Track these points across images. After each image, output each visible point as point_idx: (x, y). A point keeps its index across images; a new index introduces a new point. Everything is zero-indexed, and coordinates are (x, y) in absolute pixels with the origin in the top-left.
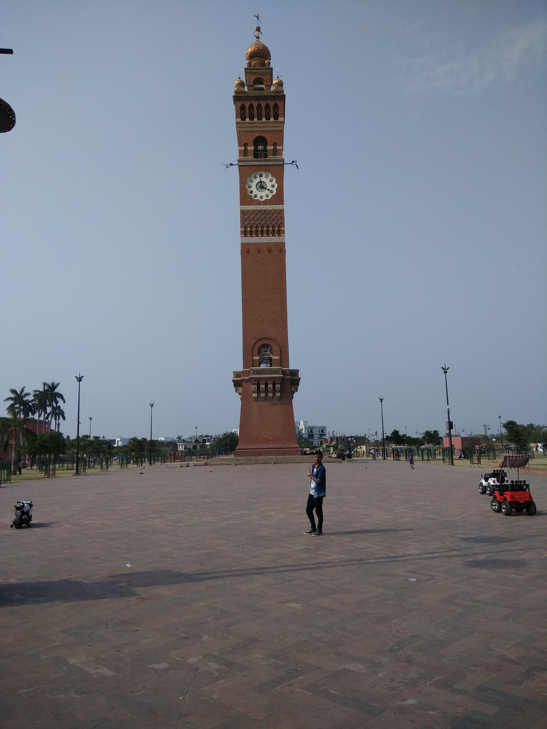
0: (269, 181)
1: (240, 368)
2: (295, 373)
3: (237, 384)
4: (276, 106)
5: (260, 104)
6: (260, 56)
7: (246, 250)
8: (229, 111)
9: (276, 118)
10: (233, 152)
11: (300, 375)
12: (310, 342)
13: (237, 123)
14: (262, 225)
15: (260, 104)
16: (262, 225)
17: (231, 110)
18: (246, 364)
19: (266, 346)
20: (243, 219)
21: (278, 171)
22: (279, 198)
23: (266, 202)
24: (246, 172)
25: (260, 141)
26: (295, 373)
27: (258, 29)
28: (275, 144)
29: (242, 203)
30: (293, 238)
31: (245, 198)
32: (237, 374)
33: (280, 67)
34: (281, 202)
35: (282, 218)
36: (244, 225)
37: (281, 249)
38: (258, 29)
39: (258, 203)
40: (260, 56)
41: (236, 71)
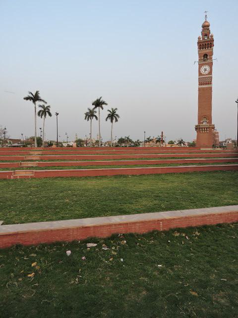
0: (207, 67)
1: (197, 124)
2: (214, 125)
3: (196, 129)
4: (211, 43)
5: (206, 44)
6: (206, 27)
7: (200, 89)
8: (196, 47)
9: (211, 47)
10: (197, 59)
11: (215, 126)
12: (217, 119)
13: (199, 51)
14: (205, 82)
15: (206, 44)
16: (205, 82)
17: (196, 47)
18: (199, 124)
19: (205, 118)
20: (199, 80)
21: (211, 65)
22: (210, 73)
23: (206, 75)
24: (200, 66)
25: (206, 56)
26: (214, 125)
27: (206, 16)
28: (210, 56)
29: (199, 76)
30: (215, 85)
31: (200, 74)
32: (196, 126)
33: (213, 30)
34: (211, 74)
35: (211, 80)
36: (199, 82)
37: (211, 88)
38: (206, 16)
39: (204, 75)
40: (206, 27)
41: (198, 33)
